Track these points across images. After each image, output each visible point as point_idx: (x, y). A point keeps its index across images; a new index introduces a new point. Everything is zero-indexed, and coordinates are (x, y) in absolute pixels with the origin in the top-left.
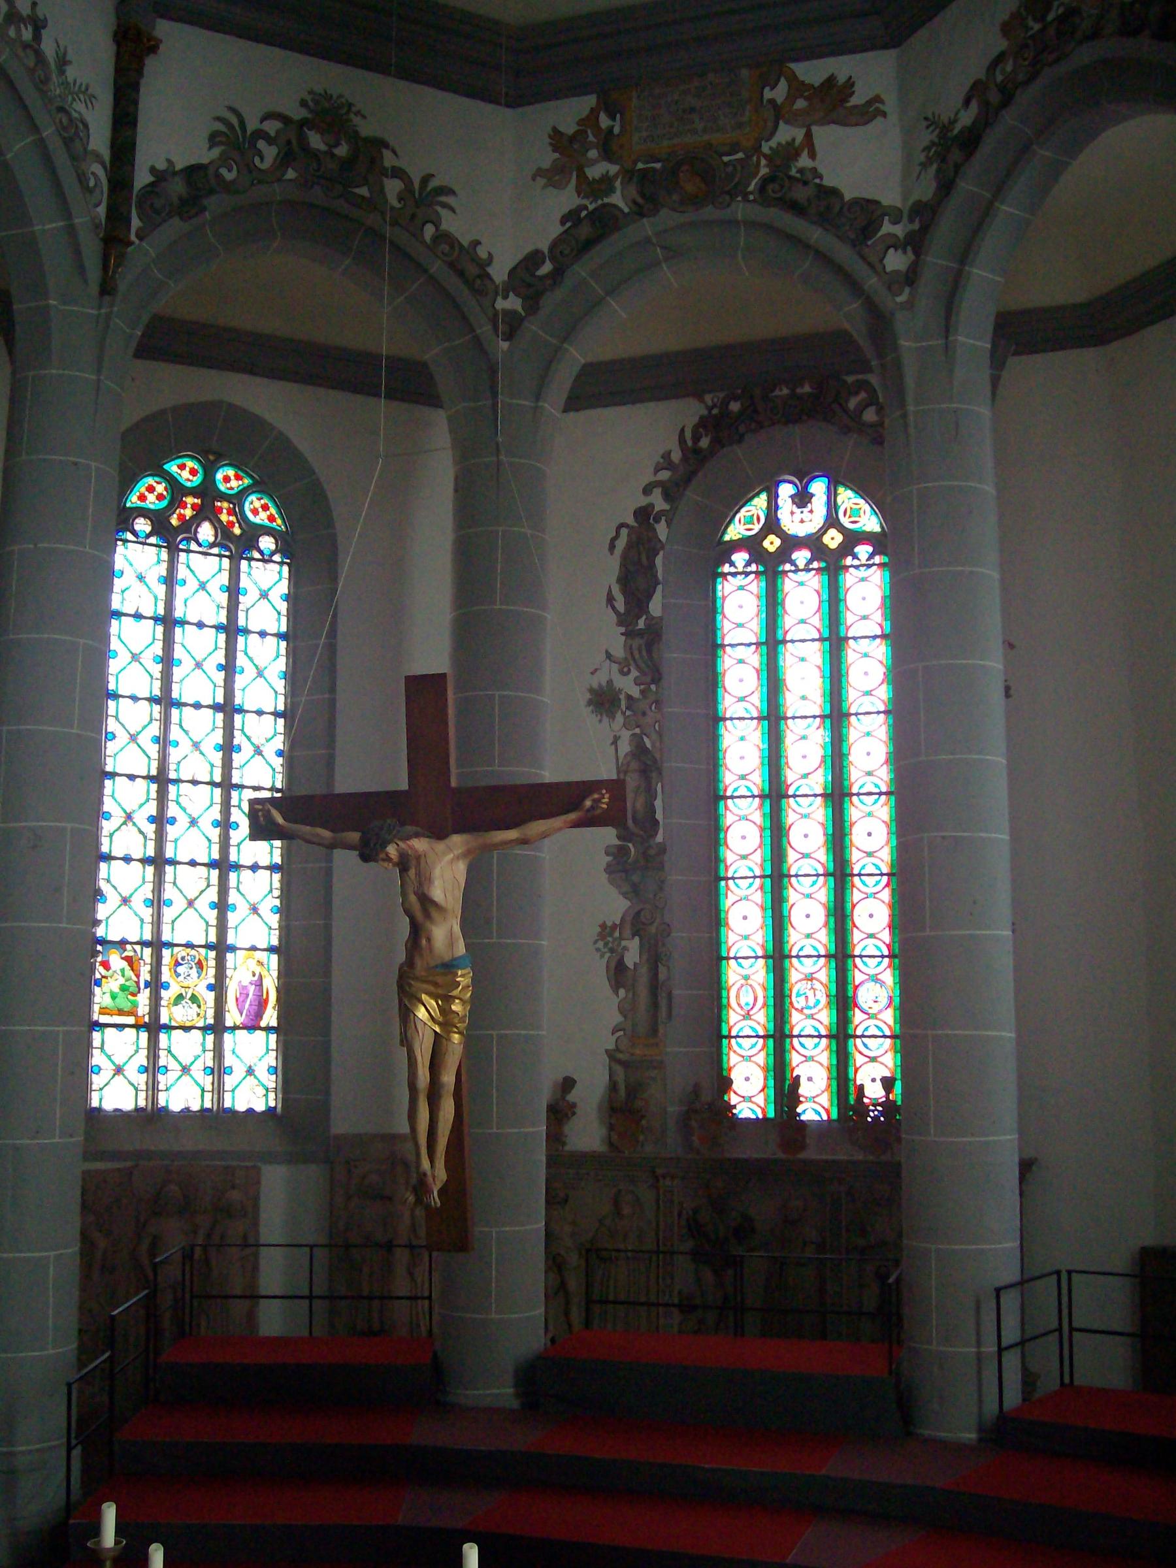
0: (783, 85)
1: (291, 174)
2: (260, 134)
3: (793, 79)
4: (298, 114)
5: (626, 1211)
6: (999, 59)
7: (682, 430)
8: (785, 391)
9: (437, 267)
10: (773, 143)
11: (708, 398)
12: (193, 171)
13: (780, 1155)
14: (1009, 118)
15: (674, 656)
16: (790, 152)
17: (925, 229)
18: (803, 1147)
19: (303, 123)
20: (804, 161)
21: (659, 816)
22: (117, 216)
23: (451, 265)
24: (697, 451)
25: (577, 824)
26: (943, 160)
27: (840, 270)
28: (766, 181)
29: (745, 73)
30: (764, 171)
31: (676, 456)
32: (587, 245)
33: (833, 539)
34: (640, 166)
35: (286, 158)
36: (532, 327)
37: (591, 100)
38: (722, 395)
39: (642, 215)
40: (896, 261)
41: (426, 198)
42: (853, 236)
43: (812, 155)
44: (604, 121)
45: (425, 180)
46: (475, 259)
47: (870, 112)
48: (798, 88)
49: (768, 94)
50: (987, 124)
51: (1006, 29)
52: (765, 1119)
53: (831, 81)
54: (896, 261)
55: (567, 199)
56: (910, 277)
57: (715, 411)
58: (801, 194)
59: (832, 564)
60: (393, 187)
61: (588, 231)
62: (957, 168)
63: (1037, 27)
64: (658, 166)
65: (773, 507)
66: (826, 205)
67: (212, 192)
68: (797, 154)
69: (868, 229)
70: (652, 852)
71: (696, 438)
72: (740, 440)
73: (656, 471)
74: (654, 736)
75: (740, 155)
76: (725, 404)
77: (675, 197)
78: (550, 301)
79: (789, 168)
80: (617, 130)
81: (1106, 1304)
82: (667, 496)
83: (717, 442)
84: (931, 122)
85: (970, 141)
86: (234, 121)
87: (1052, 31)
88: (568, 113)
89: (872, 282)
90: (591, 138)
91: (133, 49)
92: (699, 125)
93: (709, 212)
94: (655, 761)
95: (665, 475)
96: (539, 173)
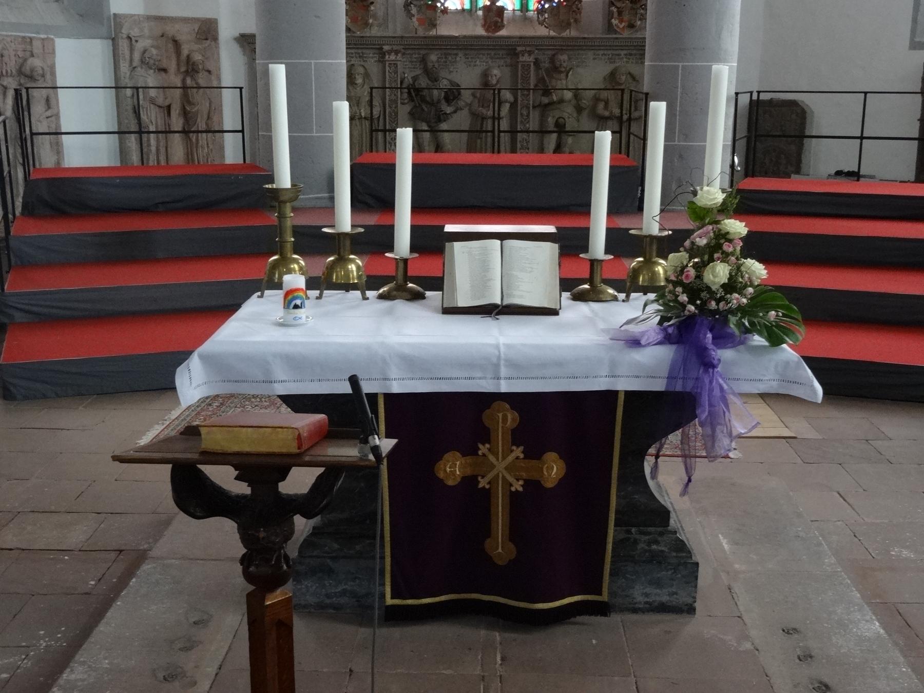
5: (359, 81)
13: (481, 32)
52: (463, 10)
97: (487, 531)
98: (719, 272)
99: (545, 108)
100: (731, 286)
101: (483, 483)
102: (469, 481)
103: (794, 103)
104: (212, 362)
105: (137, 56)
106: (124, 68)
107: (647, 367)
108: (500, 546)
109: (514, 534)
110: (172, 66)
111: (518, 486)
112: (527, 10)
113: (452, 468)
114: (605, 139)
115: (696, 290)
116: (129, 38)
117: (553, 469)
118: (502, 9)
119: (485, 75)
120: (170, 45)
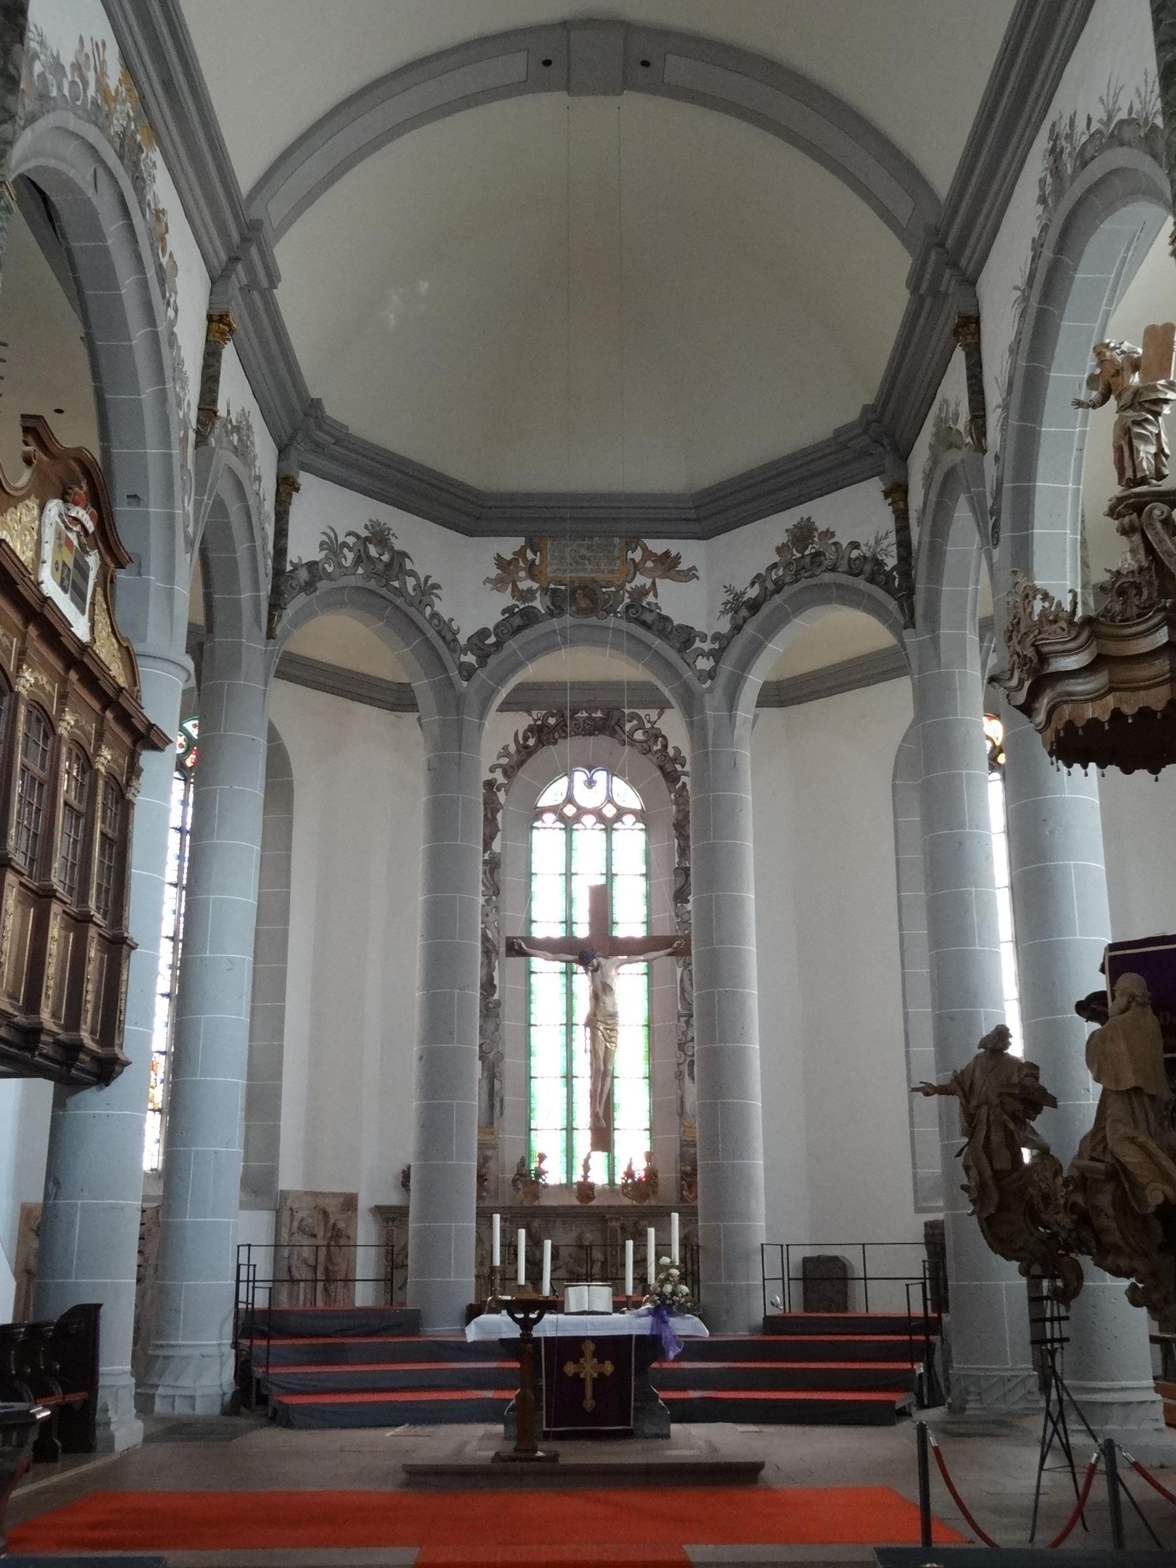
0: (639, 551)
1: (360, 571)
2: (345, 545)
3: (645, 549)
4: (364, 533)
6: (775, 566)
7: (516, 734)
8: (585, 715)
9: (431, 633)
10: (633, 585)
11: (534, 713)
12: (312, 565)
13: (576, 1202)
14: (778, 599)
15: (508, 878)
16: (642, 592)
17: (722, 650)
18: (592, 1198)
19: (367, 539)
20: (650, 598)
21: (496, 982)
22: (276, 591)
23: (439, 632)
24: (526, 747)
25: (670, 954)
26: (736, 613)
27: (669, 665)
28: (628, 607)
29: (617, 540)
30: (627, 601)
31: (512, 749)
32: (519, 629)
33: (610, 811)
34: (552, 586)
35: (358, 561)
36: (481, 674)
37: (520, 541)
38: (544, 712)
39: (552, 616)
40: (704, 664)
41: (427, 590)
42: (678, 645)
43: (656, 596)
44: (530, 555)
45: (427, 578)
46: (451, 630)
47: (690, 575)
48: (648, 554)
49: (630, 555)
50: (765, 600)
51: (779, 550)
52: (561, 1185)
53: (667, 554)
55: (506, 599)
56: (712, 675)
57: (539, 722)
58: (648, 618)
59: (608, 826)
60: (411, 582)
61: (520, 620)
62: (745, 620)
63: (799, 555)
64: (563, 588)
65: (570, 788)
66: (662, 625)
67: (321, 579)
68: (647, 593)
70: (491, 1006)
71: (526, 739)
72: (555, 743)
73: (499, 757)
74: (494, 930)
75: (613, 589)
76: (545, 718)
77: (574, 608)
78: (493, 661)
79: (641, 601)
80: (537, 562)
82: (506, 774)
83: (540, 743)
84: (729, 590)
86: (333, 536)
87: (808, 560)
89: (688, 674)
90: (521, 564)
91: (286, 486)
92: (589, 567)
93: (593, 620)
94: (494, 946)
95: (504, 761)
96: (488, 580)
97: (583, 1397)
98: (668, 1288)
100: (674, 1293)
101: (582, 1376)
102: (577, 1375)
103: (836, 1259)
104: (480, 1326)
105: (296, 1224)
106: (285, 1235)
108: (589, 1404)
109: (595, 1396)
110: (321, 1234)
111: (595, 1375)
112: (614, 1184)
113: (570, 1368)
114: (630, 1244)
115: (661, 1295)
116: (291, 1209)
117: (609, 1368)
118: (591, 1187)
119: (580, 1237)
120: (321, 1216)
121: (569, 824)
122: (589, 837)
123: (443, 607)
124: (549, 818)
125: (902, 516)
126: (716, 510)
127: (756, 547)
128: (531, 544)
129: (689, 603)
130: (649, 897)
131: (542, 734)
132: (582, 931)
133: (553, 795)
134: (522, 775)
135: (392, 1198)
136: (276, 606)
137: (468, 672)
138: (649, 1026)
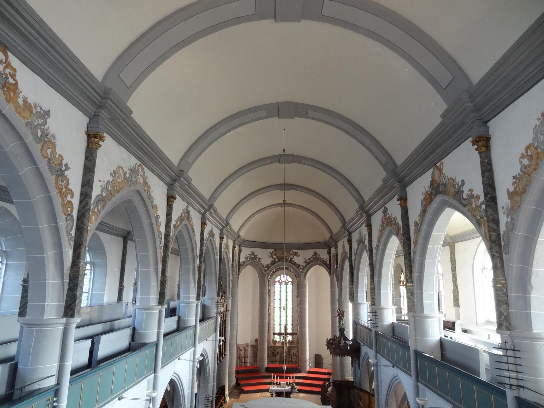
16: (292, 258)
33: (287, 281)
40: (301, 270)
41: (260, 260)
47: (299, 256)
48: (293, 252)
54: (301, 270)
55: (271, 259)
56: (302, 272)
59: (286, 284)
61: (273, 263)
66: (295, 264)
69: (299, 267)
81: (313, 360)
85: (309, 263)
88: (272, 250)
99: (289, 355)
107: (290, 391)
121: (280, 284)
122: (283, 286)
123: (262, 262)
124: (277, 282)
125: (330, 257)
126: (304, 246)
127: (308, 254)
128: (275, 250)
129: (298, 260)
130: (293, 296)
131: (277, 270)
132: (283, 331)
133: (278, 279)
134: (274, 276)
135: (254, 343)
136: (239, 270)
137: (266, 271)
138: (292, 316)
